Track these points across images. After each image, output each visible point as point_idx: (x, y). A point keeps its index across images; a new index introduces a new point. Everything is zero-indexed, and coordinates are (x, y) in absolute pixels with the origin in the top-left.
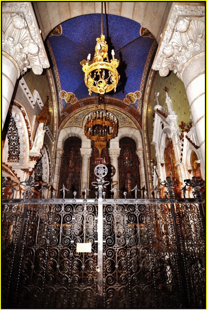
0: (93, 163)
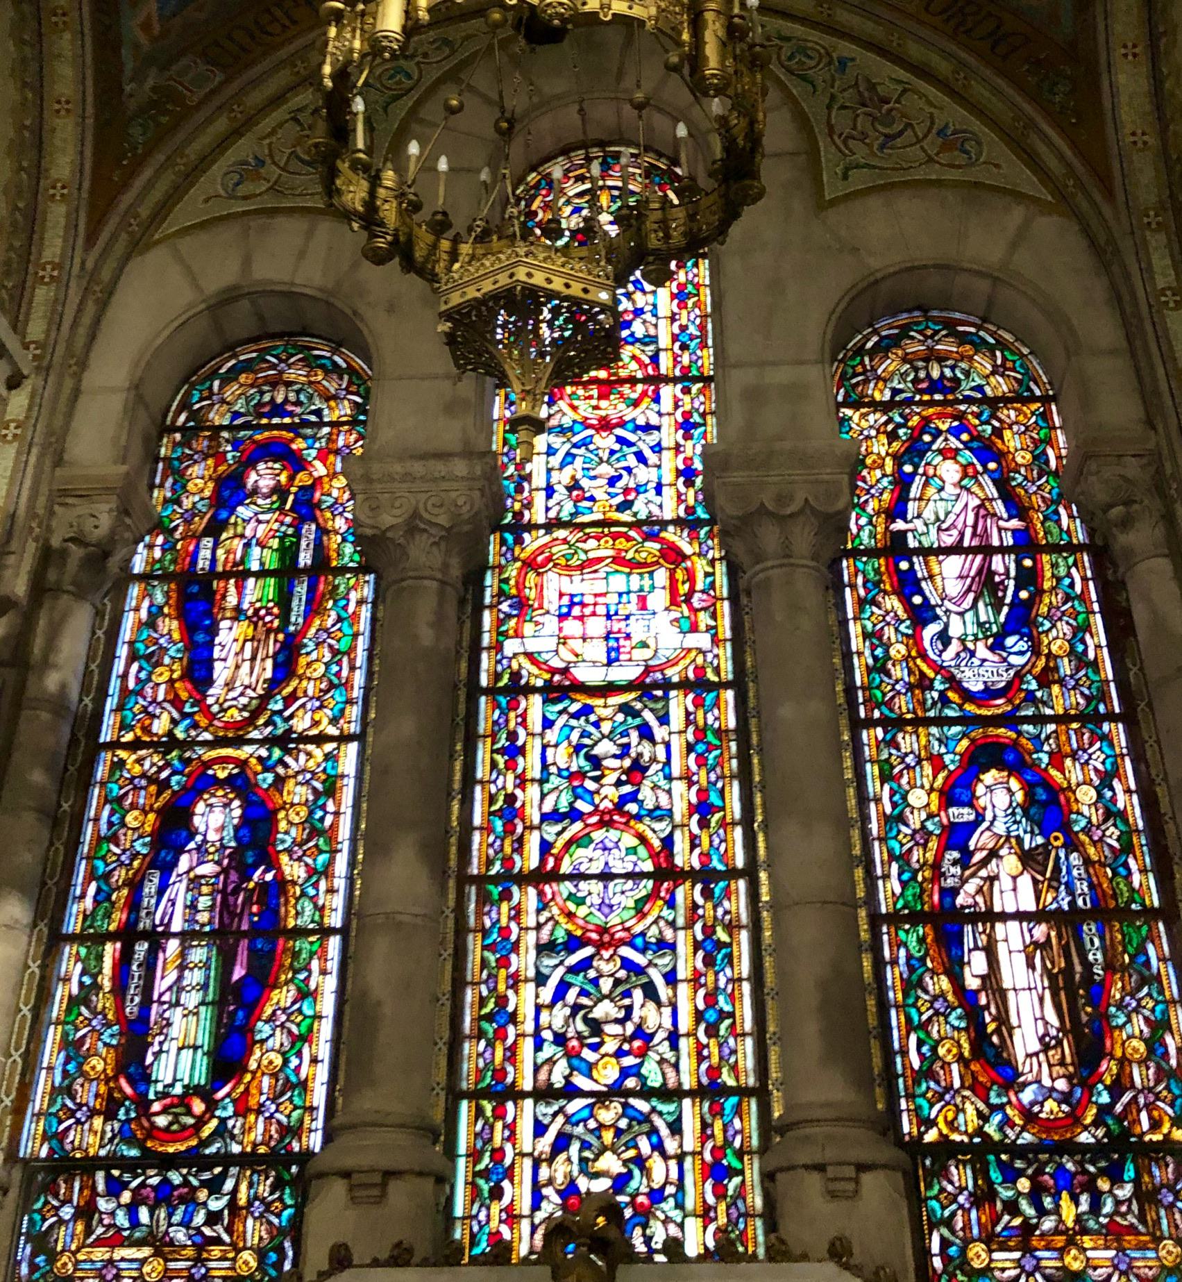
0: (510, 647)
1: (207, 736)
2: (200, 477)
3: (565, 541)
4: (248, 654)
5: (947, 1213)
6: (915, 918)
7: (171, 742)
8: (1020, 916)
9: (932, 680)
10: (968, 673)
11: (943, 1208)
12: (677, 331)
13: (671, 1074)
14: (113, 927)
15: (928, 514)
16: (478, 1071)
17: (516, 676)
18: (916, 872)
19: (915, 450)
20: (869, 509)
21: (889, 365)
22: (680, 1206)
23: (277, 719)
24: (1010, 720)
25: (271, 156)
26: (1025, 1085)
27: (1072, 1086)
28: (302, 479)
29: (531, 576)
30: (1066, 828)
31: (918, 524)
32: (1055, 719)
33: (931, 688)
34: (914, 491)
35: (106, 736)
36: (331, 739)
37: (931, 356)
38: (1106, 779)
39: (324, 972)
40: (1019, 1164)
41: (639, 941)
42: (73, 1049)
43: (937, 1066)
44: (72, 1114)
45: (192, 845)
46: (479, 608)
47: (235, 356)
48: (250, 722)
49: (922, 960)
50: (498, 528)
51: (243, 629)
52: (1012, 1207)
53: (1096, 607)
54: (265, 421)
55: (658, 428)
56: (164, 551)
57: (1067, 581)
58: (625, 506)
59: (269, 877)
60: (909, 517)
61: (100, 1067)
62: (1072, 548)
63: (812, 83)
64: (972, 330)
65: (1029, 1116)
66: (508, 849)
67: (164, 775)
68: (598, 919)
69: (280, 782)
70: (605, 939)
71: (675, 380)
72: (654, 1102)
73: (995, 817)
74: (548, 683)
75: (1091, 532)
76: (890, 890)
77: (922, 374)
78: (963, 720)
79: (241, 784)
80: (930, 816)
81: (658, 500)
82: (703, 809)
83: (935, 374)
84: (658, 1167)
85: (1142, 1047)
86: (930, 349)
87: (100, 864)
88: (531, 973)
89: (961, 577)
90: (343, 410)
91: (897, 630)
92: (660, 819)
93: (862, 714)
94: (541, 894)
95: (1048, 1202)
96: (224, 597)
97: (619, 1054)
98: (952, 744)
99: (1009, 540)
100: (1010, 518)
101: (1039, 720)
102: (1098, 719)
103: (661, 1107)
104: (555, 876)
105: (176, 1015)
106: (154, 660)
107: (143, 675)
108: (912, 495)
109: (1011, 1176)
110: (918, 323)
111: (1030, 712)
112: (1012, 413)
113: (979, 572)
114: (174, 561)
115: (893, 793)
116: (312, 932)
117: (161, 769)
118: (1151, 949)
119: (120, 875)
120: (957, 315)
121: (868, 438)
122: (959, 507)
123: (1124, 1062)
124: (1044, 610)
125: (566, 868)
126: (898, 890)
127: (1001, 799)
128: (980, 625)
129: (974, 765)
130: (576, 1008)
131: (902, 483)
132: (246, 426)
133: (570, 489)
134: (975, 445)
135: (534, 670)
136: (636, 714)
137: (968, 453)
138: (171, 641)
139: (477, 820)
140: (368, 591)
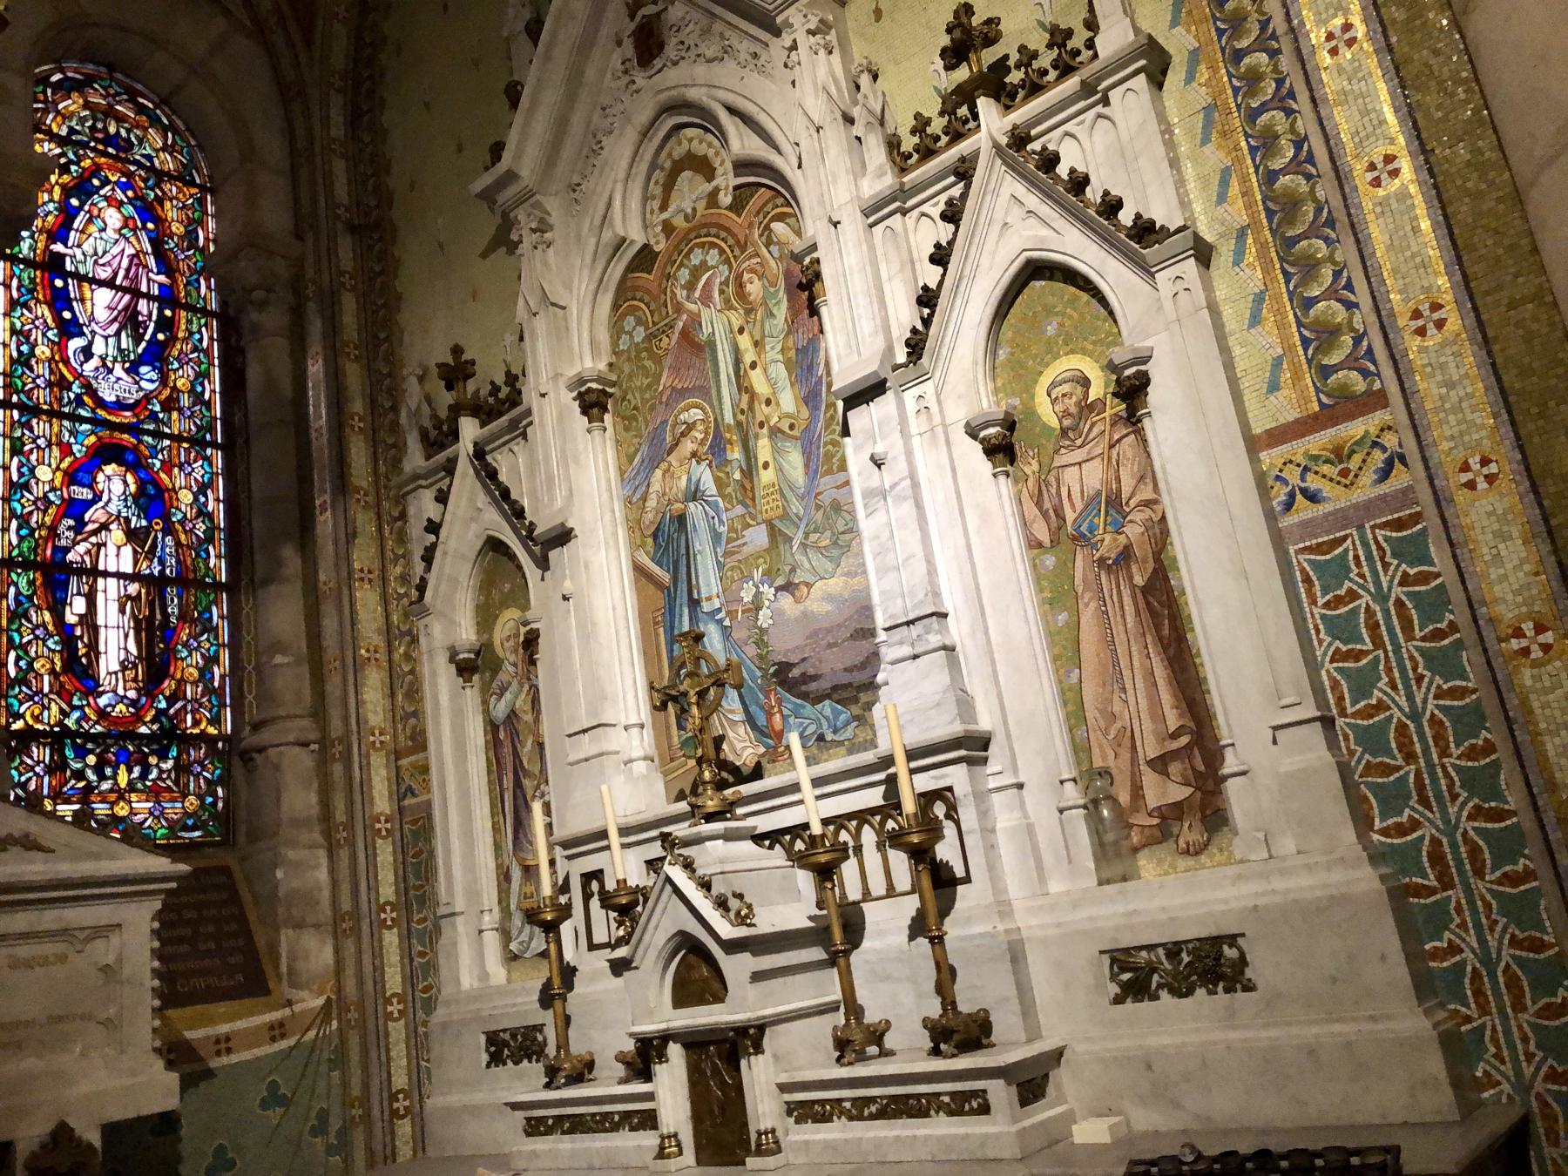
5: (23, 779)
6: (27, 565)
8: (119, 575)
9: (71, 384)
11: (21, 775)
18: (32, 531)
19: (83, 188)
21: (71, 104)
26: (104, 692)
27: (140, 695)
30: (166, 518)
31: (78, 252)
32: (171, 437)
37: (110, 113)
38: (203, 488)
40: (90, 746)
43: (31, 676)
49: (30, 598)
52: (79, 775)
57: (197, 336)
62: (205, 312)
65: (102, 714)
73: (110, 500)
75: (223, 303)
77: (100, 125)
80: (53, 489)
85: (196, 674)
86: (111, 106)
89: (109, 307)
91: (44, 335)
95: (108, 771)
98: (80, 438)
101: (159, 435)
102: (204, 444)
108: (75, 226)
109: (81, 753)
110: (102, 79)
111: (151, 427)
113: (126, 308)
115: (21, 465)
118: (214, 609)
120: (139, 87)
122: (116, 250)
123: (182, 682)
126: (15, 541)
128: (120, 350)
134: (139, 203)
137: (131, 208)
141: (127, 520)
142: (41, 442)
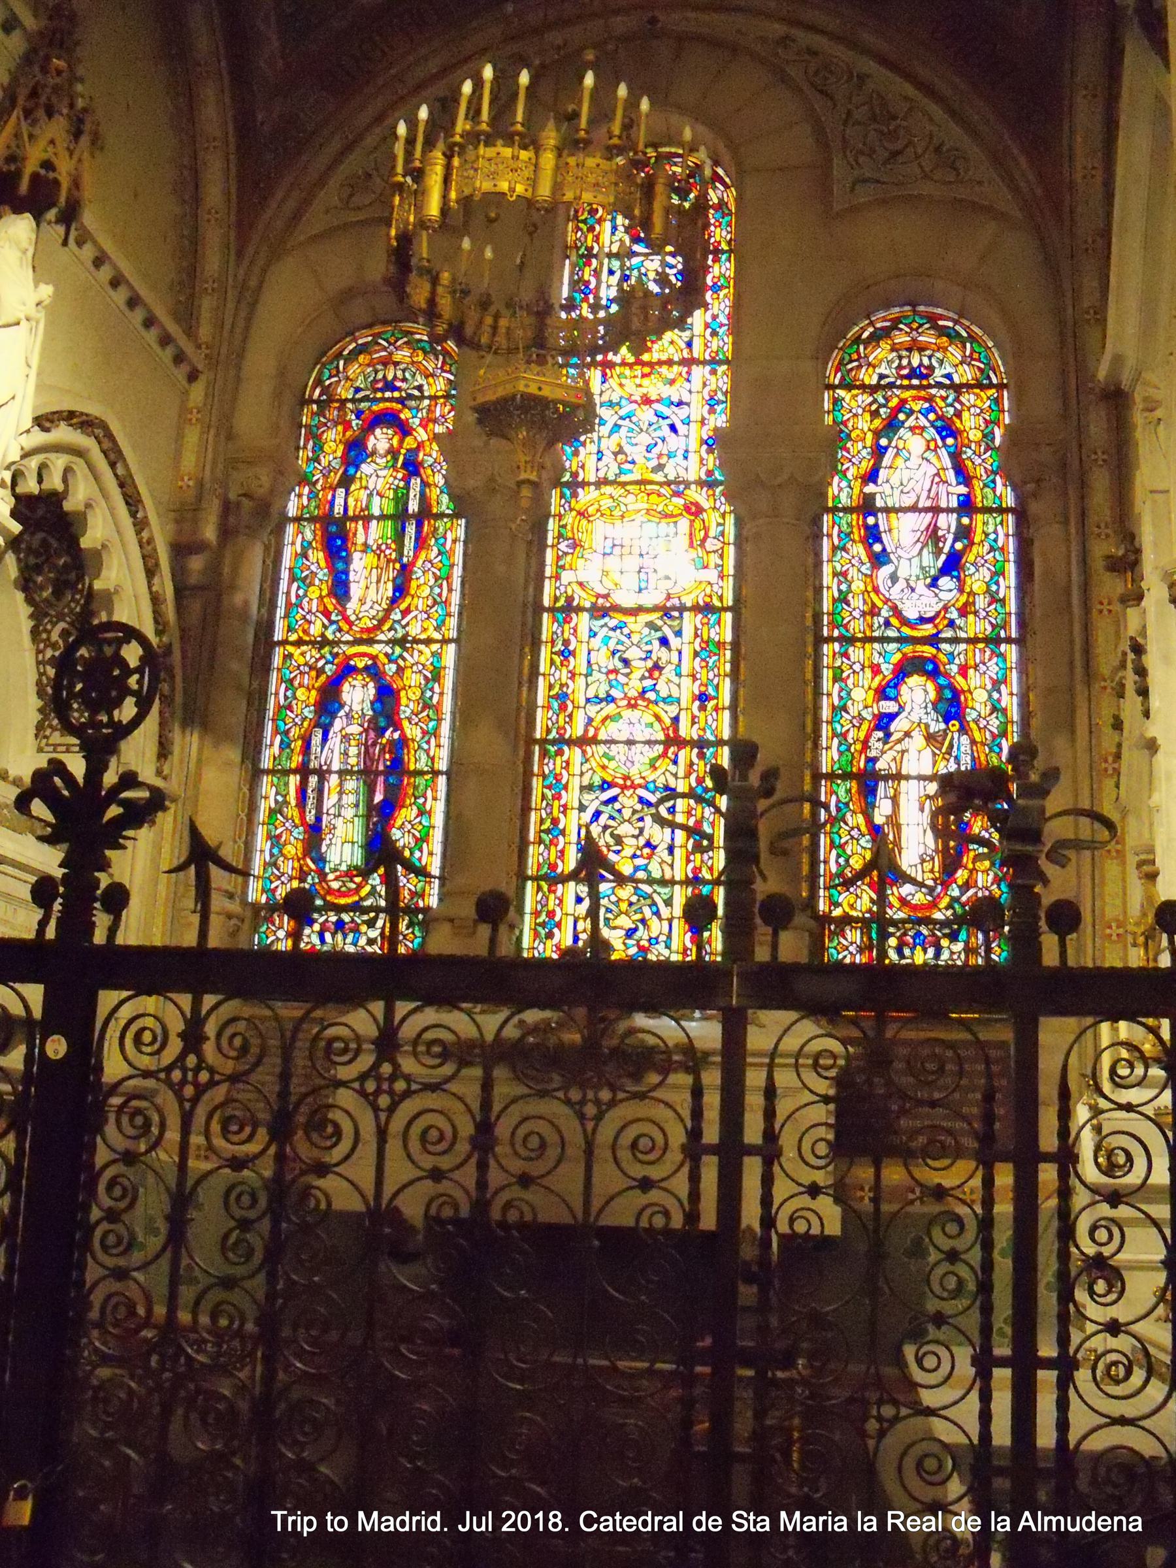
0: (566, 576)
1: (347, 638)
2: (333, 441)
3: (612, 497)
4: (374, 579)
6: (846, 776)
7: (323, 642)
8: (921, 778)
10: (908, 603)
12: (709, 320)
13: (667, 869)
14: (294, 765)
15: (895, 480)
16: (539, 865)
17: (570, 599)
19: (891, 426)
20: (849, 475)
21: (881, 352)
22: (668, 947)
23: (397, 626)
24: (934, 640)
25: (377, 170)
28: (410, 443)
29: (584, 522)
31: (886, 488)
32: (969, 641)
33: (879, 615)
34: (886, 461)
35: (278, 636)
36: (437, 641)
39: (435, 799)
41: (651, 786)
42: (275, 839)
44: (279, 878)
45: (342, 713)
46: (543, 546)
47: (355, 340)
48: (378, 628)
49: (847, 804)
50: (557, 483)
51: (371, 559)
53: (1012, 557)
54: (379, 395)
55: (688, 404)
56: (309, 499)
57: (993, 536)
58: (660, 467)
59: (396, 735)
60: (880, 481)
61: (293, 852)
62: (1001, 510)
63: (832, 99)
64: (950, 324)
66: (561, 723)
67: (320, 664)
68: (623, 770)
69: (400, 670)
70: (628, 784)
71: (704, 363)
72: (656, 887)
74: (594, 605)
75: (1018, 497)
76: (829, 759)
78: (901, 640)
79: (374, 671)
81: (684, 463)
82: (703, 698)
83: (915, 363)
84: (654, 923)
86: (914, 340)
87: (281, 724)
88: (576, 805)
90: (438, 386)
92: (672, 703)
93: (825, 634)
94: (584, 752)
96: (355, 534)
97: (634, 856)
99: (954, 503)
100: (959, 484)
101: (955, 641)
103: (659, 889)
104: (594, 741)
105: (339, 822)
106: (307, 582)
107: (301, 592)
110: (906, 317)
112: (972, 397)
114: (318, 507)
115: (841, 690)
116: (427, 773)
117: (317, 660)
119: (295, 732)
120: (939, 311)
121: (856, 415)
124: (971, 558)
125: (602, 736)
126: (836, 758)
127: (919, 696)
128: (922, 568)
129: (902, 672)
130: (606, 827)
131: (879, 452)
132: (366, 399)
133: (615, 454)
135: (583, 594)
136: (658, 629)
137: (932, 430)
138: (319, 567)
139: (540, 702)
140: (461, 532)
141: (927, 726)
142: (857, 667)
